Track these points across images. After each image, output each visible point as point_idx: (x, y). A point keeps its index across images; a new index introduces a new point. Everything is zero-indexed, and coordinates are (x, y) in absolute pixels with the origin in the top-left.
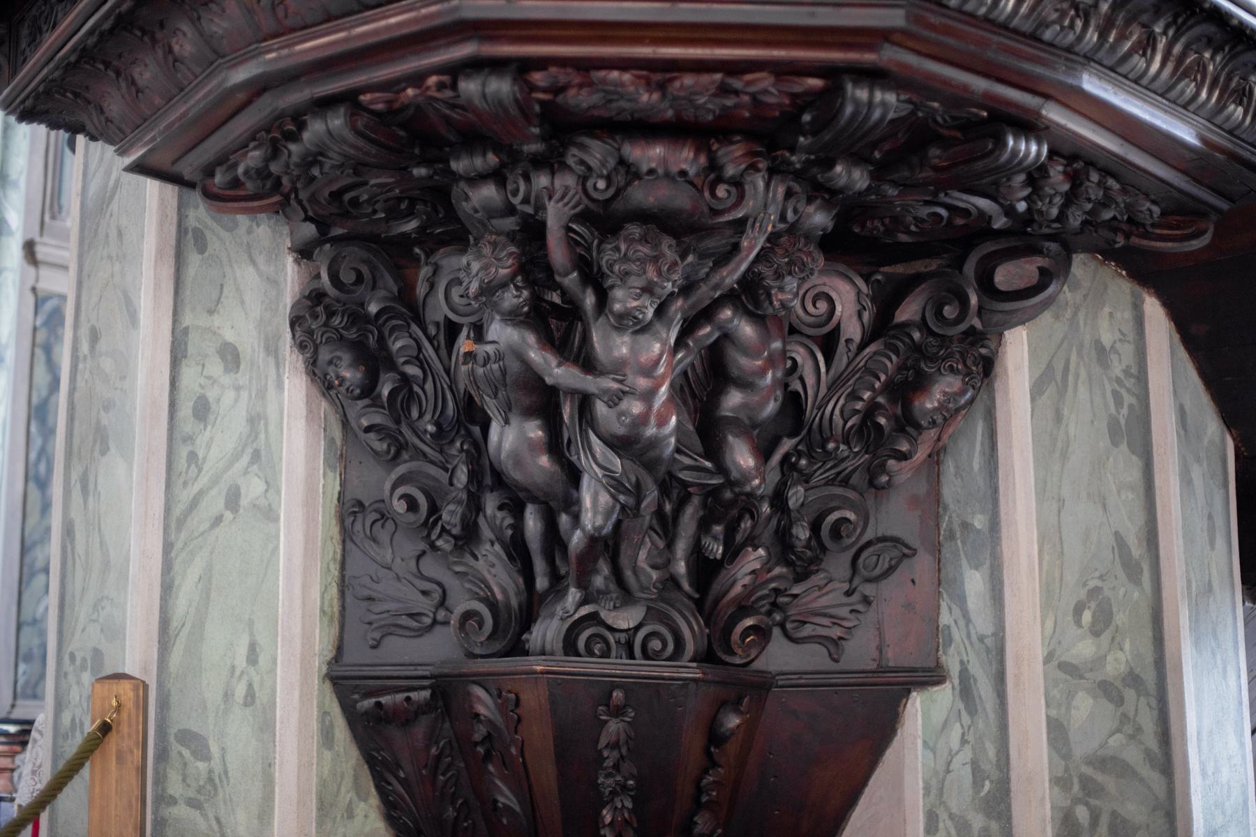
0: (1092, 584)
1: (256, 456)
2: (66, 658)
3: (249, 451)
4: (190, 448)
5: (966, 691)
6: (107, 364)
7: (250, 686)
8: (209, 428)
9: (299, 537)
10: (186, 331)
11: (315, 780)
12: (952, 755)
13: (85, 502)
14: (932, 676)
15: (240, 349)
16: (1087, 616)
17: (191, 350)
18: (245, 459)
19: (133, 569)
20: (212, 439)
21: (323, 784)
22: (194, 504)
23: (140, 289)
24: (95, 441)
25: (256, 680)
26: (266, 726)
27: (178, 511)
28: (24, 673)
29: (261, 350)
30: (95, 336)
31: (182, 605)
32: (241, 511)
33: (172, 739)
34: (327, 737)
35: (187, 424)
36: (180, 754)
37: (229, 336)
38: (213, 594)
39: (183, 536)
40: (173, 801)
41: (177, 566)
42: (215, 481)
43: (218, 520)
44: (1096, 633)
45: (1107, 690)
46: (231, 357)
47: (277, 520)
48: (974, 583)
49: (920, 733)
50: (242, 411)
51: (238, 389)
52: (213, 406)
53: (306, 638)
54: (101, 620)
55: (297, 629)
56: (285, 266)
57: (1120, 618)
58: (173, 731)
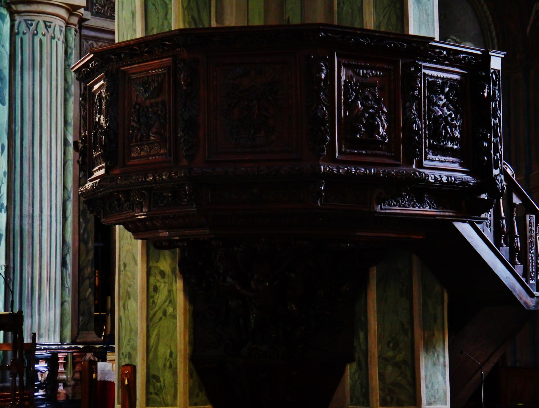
1: (170, 301)
2: (121, 354)
3: (168, 300)
4: (153, 299)
5: (359, 365)
6: (129, 274)
7: (170, 363)
8: (158, 294)
9: (182, 323)
10: (150, 267)
11: (188, 387)
13: (125, 312)
14: (351, 360)
15: (165, 272)
16: (391, 345)
17: (152, 273)
18: (168, 302)
20: (159, 297)
21: (190, 388)
22: (154, 314)
23: (137, 255)
24: (126, 295)
26: (175, 374)
27: (150, 316)
28: (82, 320)
29: (171, 272)
31: (152, 341)
32: (167, 316)
33: (151, 377)
34: (191, 376)
35: (152, 293)
36: (153, 381)
38: (160, 339)
39: (152, 323)
40: (151, 394)
41: (151, 331)
42: (160, 308)
43: (161, 319)
44: (394, 349)
45: (396, 365)
46: (163, 274)
47: (176, 318)
48: (362, 335)
49: (349, 375)
51: (165, 283)
52: (159, 288)
53: (185, 350)
54: (130, 345)
55: (182, 347)
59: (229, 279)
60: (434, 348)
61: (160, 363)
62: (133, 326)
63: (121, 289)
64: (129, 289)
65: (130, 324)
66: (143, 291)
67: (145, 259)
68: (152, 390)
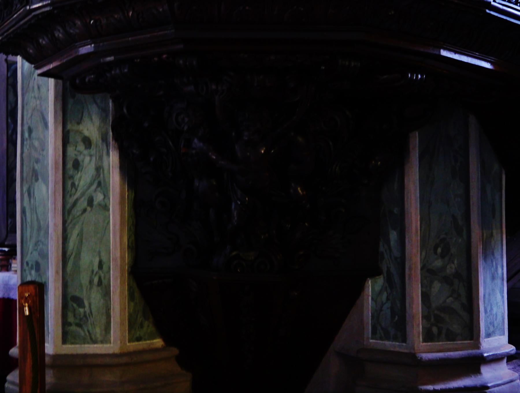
0: (442, 236)
1: (99, 184)
2: (25, 264)
3: (96, 182)
4: (72, 181)
5: (389, 280)
6: (36, 143)
7: (100, 278)
8: (79, 173)
9: (118, 217)
10: (68, 132)
11: (127, 314)
12: (383, 304)
13: (30, 200)
14: (375, 273)
15: (91, 139)
16: (439, 250)
17: (71, 140)
19: (51, 230)
20: (81, 177)
21: (130, 315)
23: (48, 113)
24: (32, 176)
25: (102, 275)
26: (107, 294)
27: (68, 206)
28: (11, 223)
29: (100, 139)
30: (30, 131)
32: (94, 207)
33: (69, 299)
34: (131, 297)
35: (71, 172)
36: (72, 306)
37: (86, 133)
38: (84, 241)
39: (71, 217)
40: (70, 324)
41: (69, 230)
42: (83, 194)
43: (85, 211)
44: (442, 256)
45: (447, 280)
46: (87, 142)
48: (393, 236)
49: (370, 294)
50: (92, 167)
51: (91, 156)
52: (81, 163)
53: (122, 258)
54: (38, 250)
55: (118, 254)
56: (109, 104)
57: (453, 250)
58: (69, 297)
59: (196, 143)
60: (493, 254)
61: (84, 279)
62: (42, 223)
63: (25, 167)
64: (36, 167)
65: (38, 219)
66: (56, 168)
67: (60, 118)
68: (71, 319)
